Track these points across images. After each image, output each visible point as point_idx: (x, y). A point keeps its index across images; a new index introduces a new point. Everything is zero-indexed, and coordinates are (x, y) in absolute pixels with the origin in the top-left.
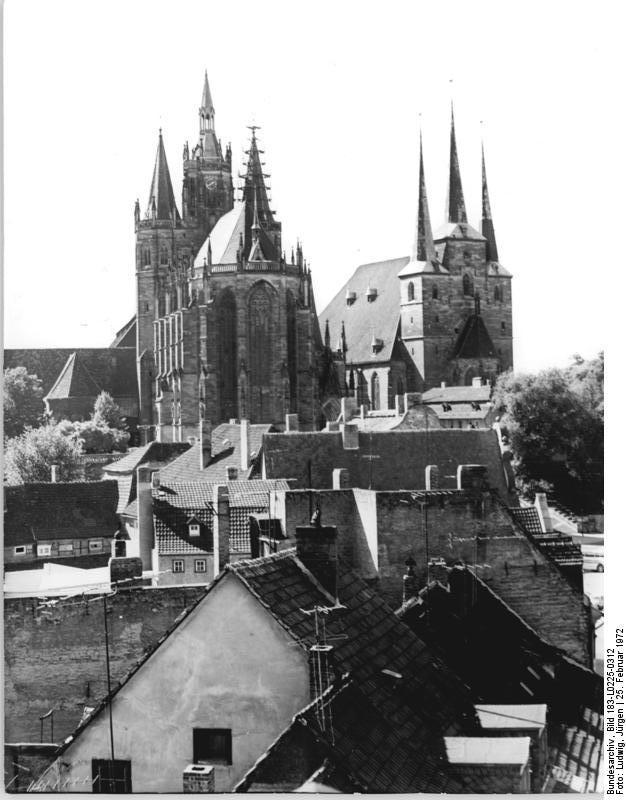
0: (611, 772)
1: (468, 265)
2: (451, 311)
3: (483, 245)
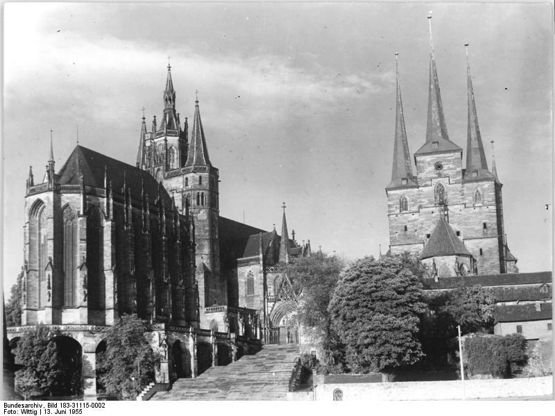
0: (19, 406)
1: (440, 175)
2: (421, 220)
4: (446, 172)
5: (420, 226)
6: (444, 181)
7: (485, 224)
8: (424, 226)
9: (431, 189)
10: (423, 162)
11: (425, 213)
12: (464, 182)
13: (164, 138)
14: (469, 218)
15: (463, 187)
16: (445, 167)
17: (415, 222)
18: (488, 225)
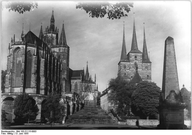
1: (136, 60)
4: (138, 59)
5: (129, 74)
6: (137, 62)
7: (148, 75)
8: (131, 74)
9: (133, 63)
10: (131, 55)
11: (131, 70)
12: (143, 62)
13: (51, 34)
14: (143, 73)
15: (142, 64)
16: (138, 57)
17: (128, 73)
18: (149, 76)
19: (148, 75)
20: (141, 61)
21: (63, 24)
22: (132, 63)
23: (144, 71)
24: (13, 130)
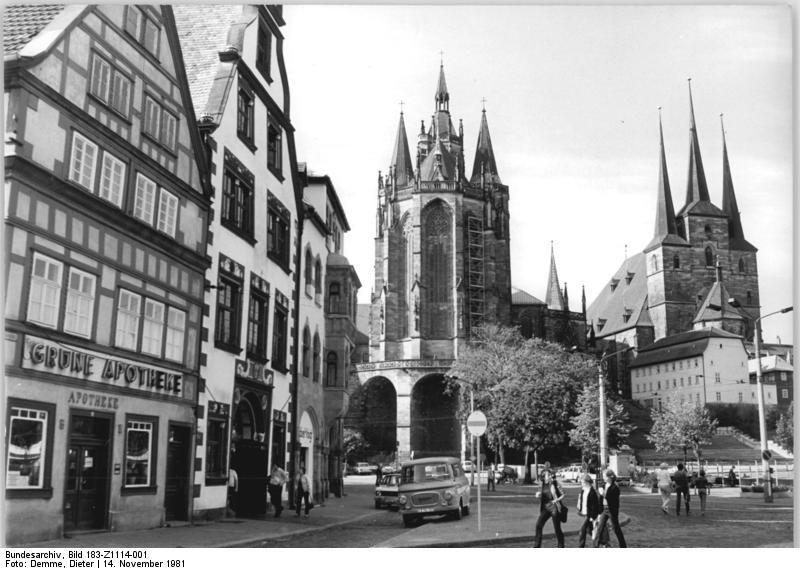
1: (710, 238)
2: (693, 280)
3: (725, 221)
9: (703, 250)
11: (697, 274)
14: (735, 285)
16: (714, 231)
19: (749, 293)
20: (726, 243)
21: (484, 111)
22: (697, 250)
23: (738, 278)
24: (52, 550)
